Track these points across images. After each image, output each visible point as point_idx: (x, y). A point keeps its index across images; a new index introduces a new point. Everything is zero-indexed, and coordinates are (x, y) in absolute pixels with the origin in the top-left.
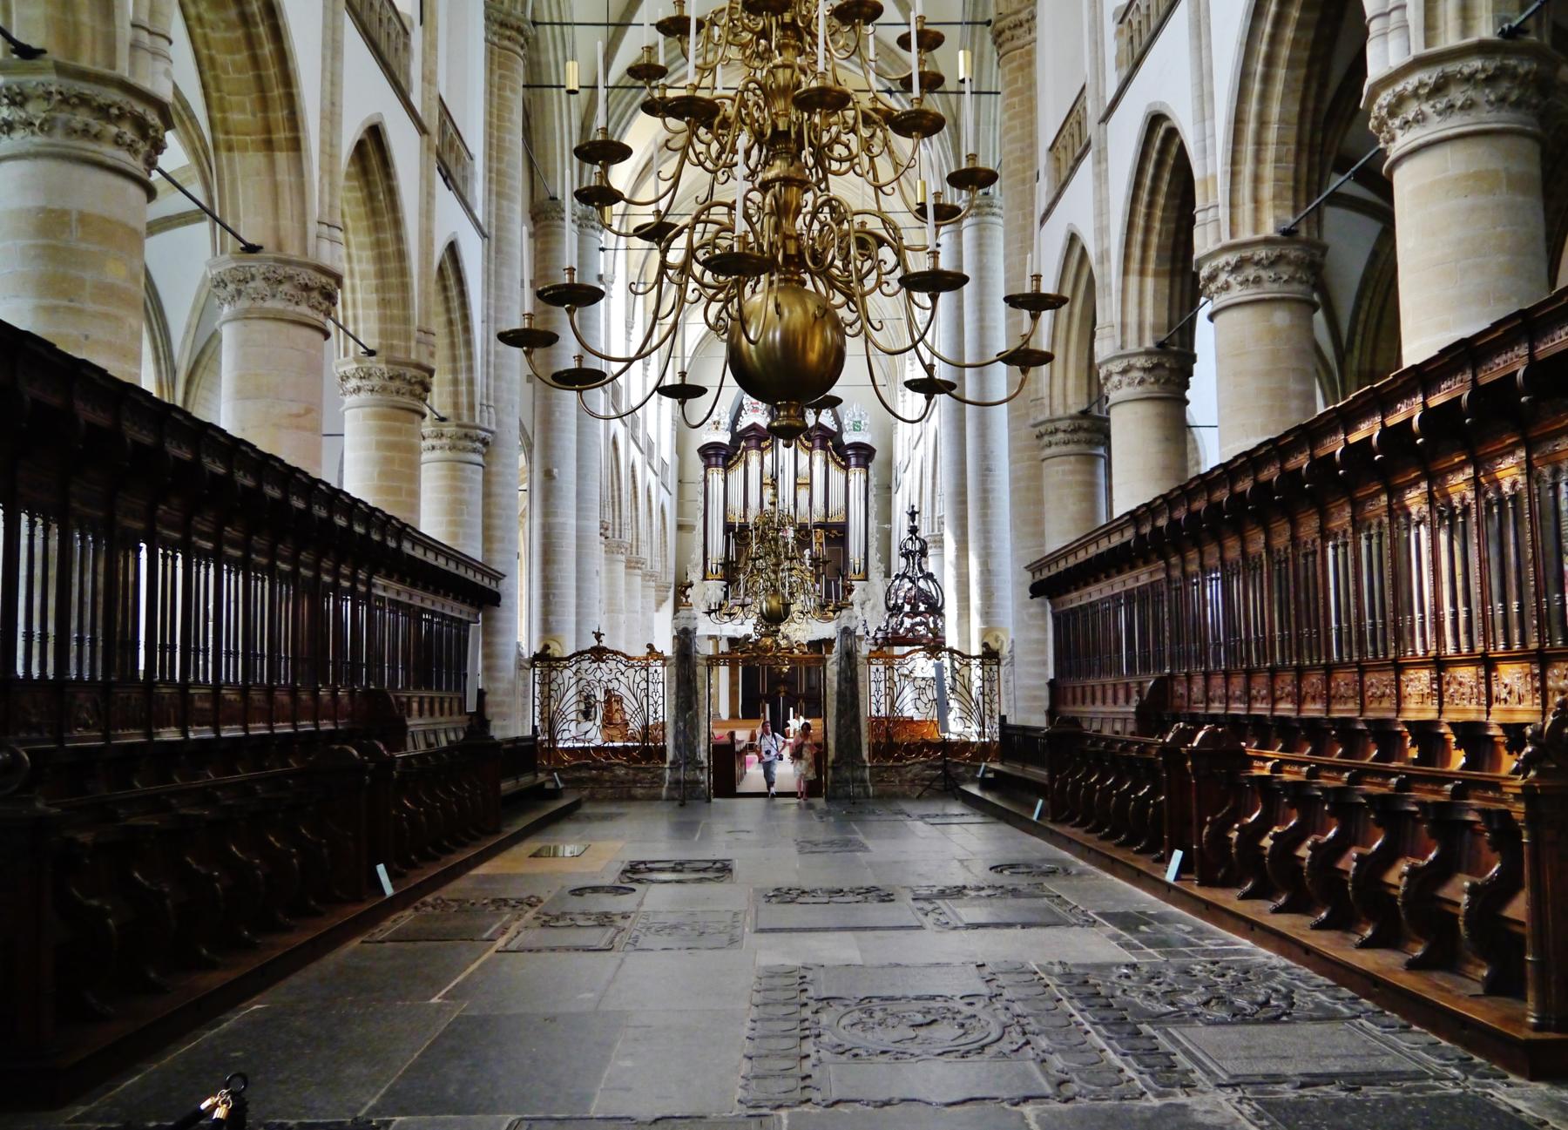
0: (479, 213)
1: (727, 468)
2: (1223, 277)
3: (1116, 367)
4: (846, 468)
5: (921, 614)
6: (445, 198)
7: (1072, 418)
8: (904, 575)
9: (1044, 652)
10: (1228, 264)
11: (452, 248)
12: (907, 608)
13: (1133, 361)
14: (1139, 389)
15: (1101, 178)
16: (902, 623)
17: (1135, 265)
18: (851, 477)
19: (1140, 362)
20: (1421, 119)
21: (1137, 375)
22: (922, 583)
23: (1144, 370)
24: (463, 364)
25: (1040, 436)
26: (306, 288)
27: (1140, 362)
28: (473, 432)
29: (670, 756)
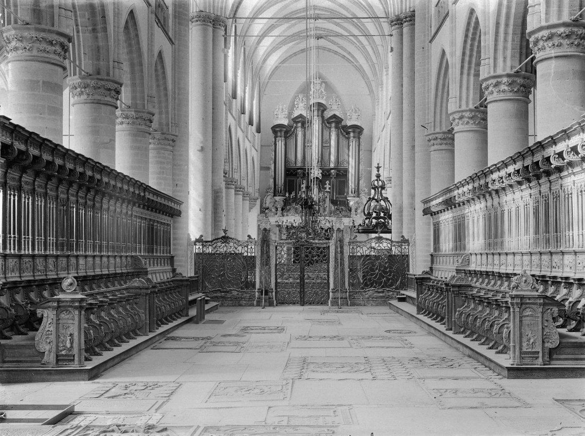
0: (170, 34)
1: (286, 138)
2: (491, 89)
3: (457, 116)
4: (348, 138)
5: (381, 218)
6: (158, 31)
7: (444, 133)
8: (373, 199)
9: (429, 240)
10: (492, 83)
11: (160, 54)
12: (374, 215)
13: (464, 114)
14: (467, 126)
15: (453, 29)
16: (372, 222)
17: (465, 71)
18: (351, 144)
19: (467, 114)
20: (543, 48)
21: (466, 120)
22: (382, 203)
23: (469, 118)
24: (163, 105)
25: (429, 140)
26: (109, 90)
27: (467, 114)
28: (168, 137)
29: (257, 286)
